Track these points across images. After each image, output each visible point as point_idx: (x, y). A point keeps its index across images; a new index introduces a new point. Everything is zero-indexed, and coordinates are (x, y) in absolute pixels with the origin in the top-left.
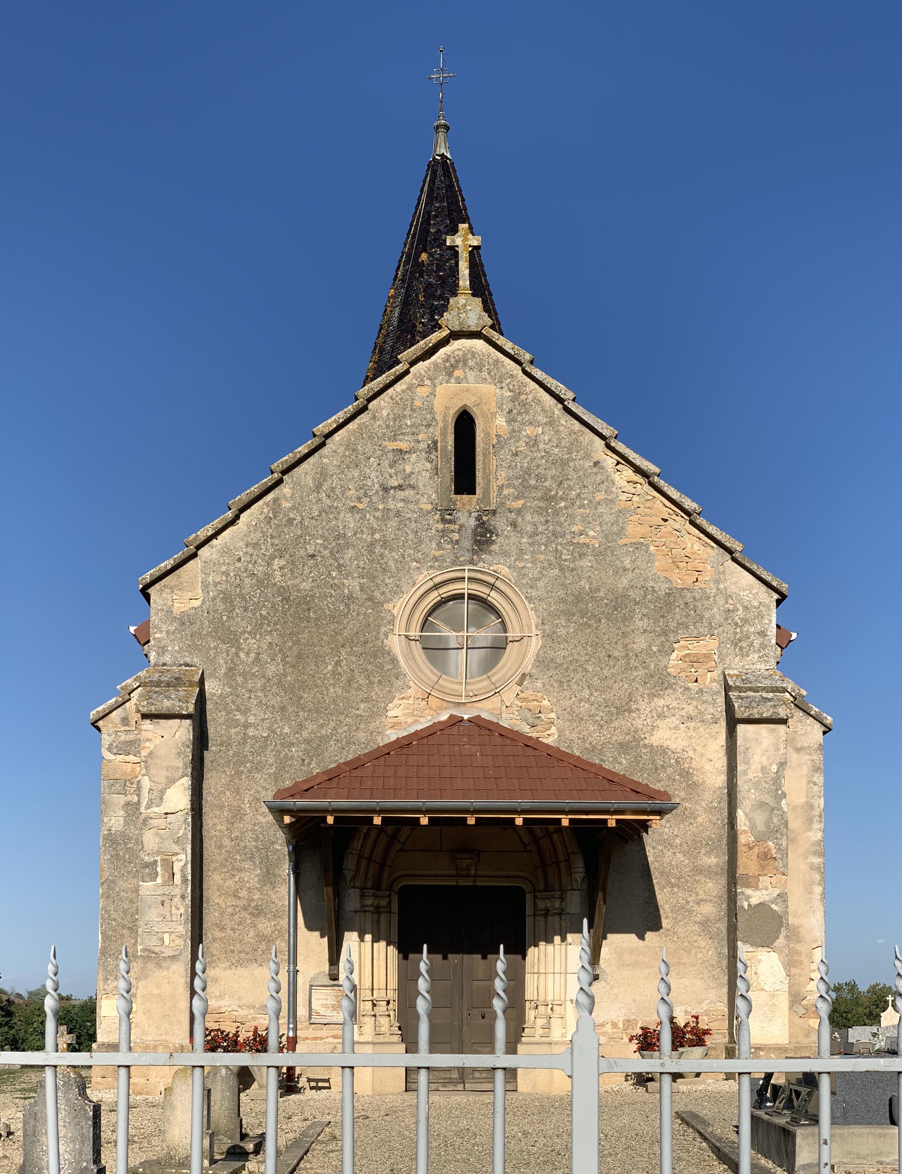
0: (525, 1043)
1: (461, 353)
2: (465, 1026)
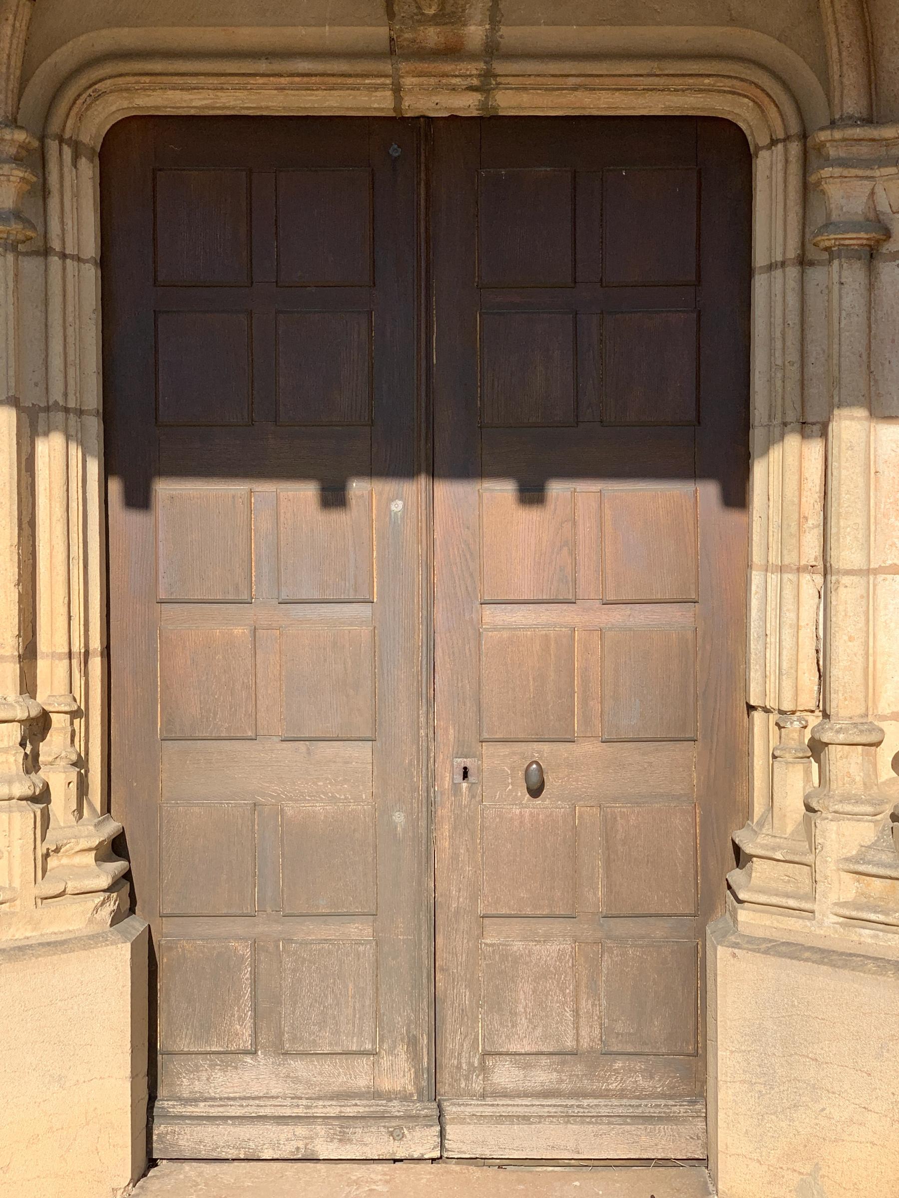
2: (444, 831)
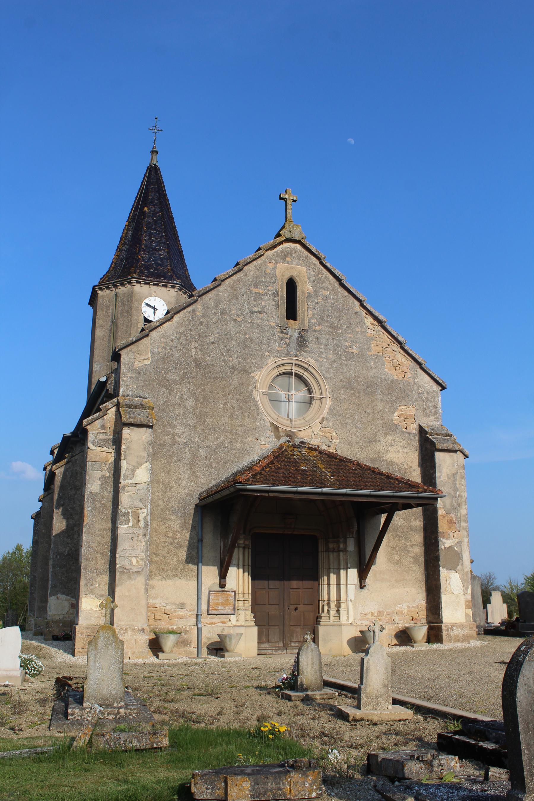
0: (323, 625)
1: (289, 250)
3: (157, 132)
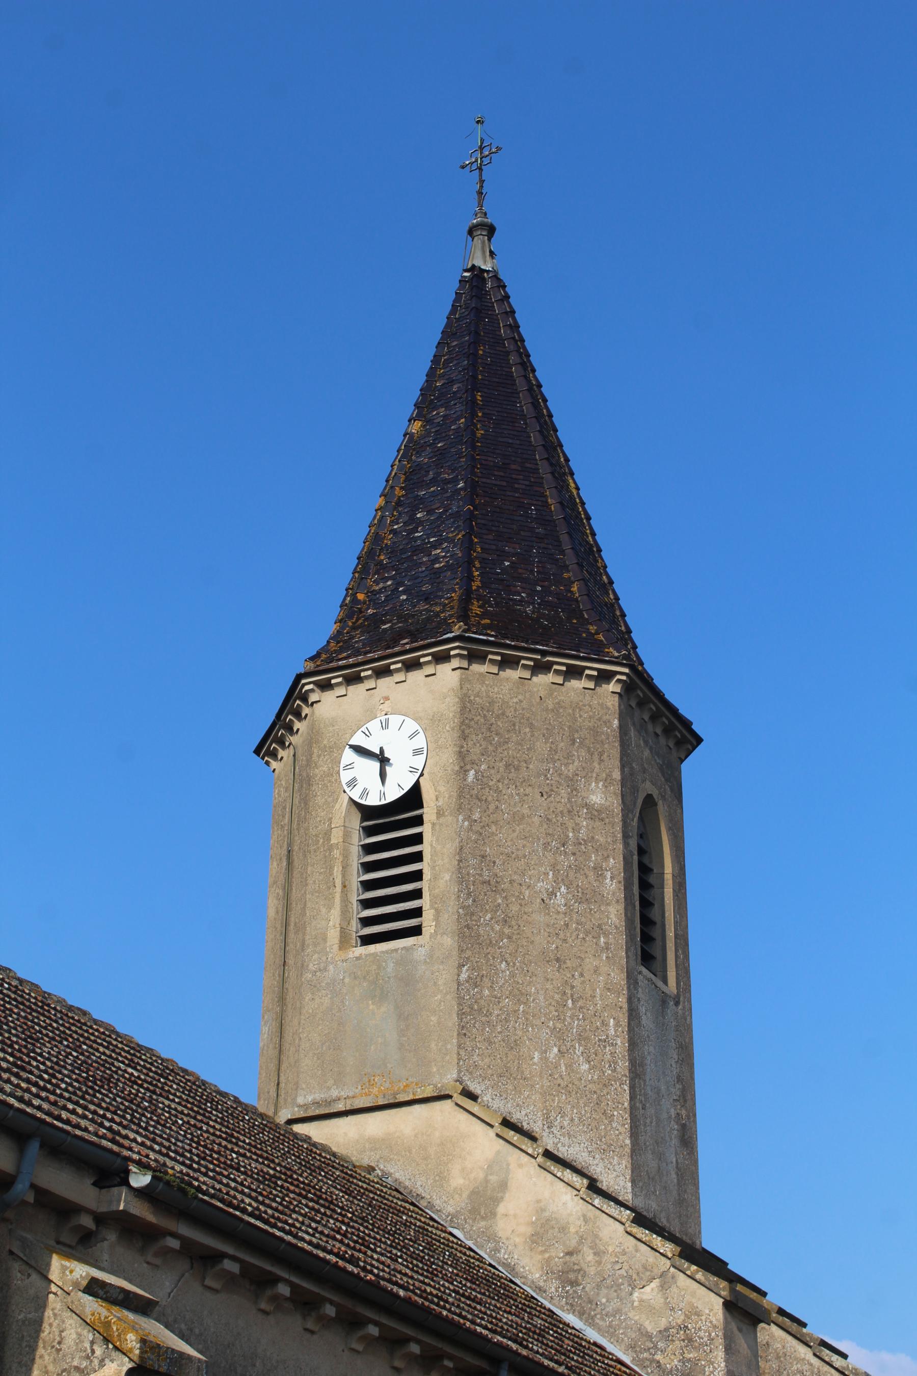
3: (486, 161)
